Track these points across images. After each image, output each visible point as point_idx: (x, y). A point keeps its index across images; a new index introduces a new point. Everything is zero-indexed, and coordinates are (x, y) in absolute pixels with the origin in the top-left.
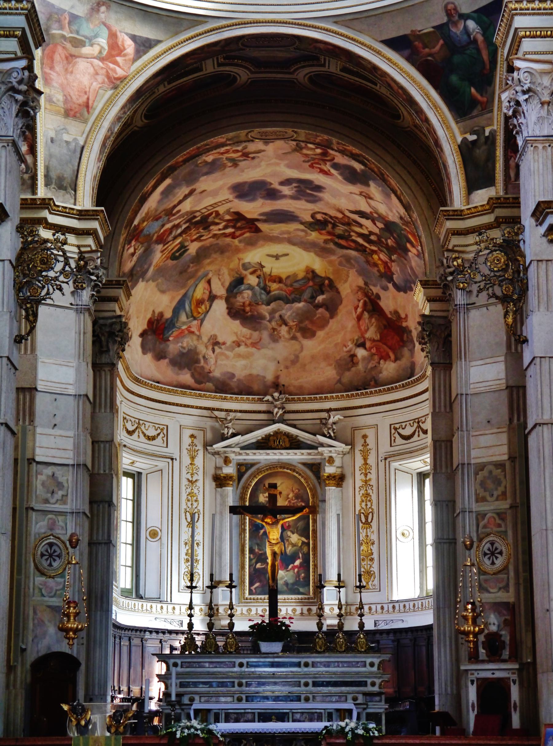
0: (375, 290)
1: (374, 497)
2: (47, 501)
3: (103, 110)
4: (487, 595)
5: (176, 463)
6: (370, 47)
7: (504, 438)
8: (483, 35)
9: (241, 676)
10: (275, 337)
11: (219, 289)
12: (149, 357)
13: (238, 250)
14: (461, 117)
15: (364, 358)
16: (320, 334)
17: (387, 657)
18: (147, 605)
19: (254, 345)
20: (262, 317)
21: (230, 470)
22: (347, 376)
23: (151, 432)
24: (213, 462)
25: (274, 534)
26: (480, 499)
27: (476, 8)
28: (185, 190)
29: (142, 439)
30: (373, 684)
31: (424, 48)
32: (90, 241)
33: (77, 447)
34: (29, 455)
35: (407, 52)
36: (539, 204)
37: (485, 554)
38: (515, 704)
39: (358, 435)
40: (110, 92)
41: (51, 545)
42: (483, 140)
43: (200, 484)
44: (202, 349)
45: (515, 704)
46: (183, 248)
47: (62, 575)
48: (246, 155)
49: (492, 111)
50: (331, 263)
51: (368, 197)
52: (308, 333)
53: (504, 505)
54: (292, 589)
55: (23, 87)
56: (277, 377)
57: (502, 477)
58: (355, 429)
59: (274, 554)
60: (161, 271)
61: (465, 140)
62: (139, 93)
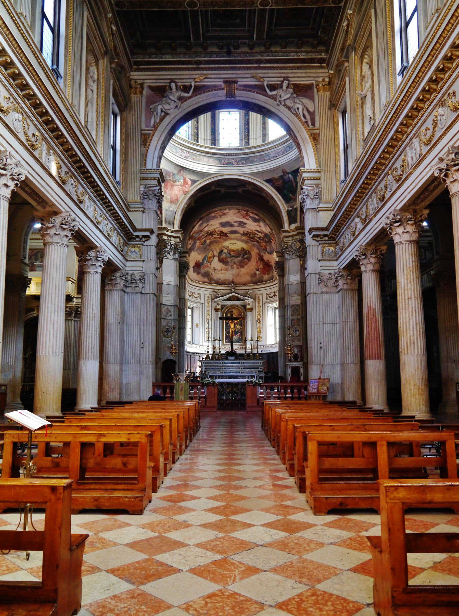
0: (262, 254)
1: (261, 315)
2: (166, 316)
3: (182, 201)
5: (203, 305)
6: (260, 182)
7: (299, 297)
9: (223, 366)
10: (232, 268)
11: (216, 253)
12: (195, 274)
13: (221, 242)
15: (258, 274)
16: (246, 267)
17: (265, 361)
18: (195, 346)
19: (226, 270)
20: (229, 262)
21: (219, 307)
22: (254, 279)
23: (196, 296)
24: (214, 304)
25: (232, 326)
26: (292, 315)
27: (291, 171)
28: (206, 224)
29: (194, 298)
30: (261, 368)
32: (178, 240)
33: (174, 300)
34: (161, 303)
35: (271, 184)
36: (310, 229)
39: (257, 296)
40: (184, 196)
41: (167, 328)
43: (210, 311)
44: (211, 271)
46: (205, 241)
47: (171, 337)
48: (224, 214)
50: (249, 246)
51: (260, 226)
52: (242, 266)
53: (299, 317)
54: (238, 341)
55: (159, 195)
56: (233, 280)
58: (256, 295)
59: (232, 331)
60: (199, 248)
61: (288, 209)
62: (192, 196)
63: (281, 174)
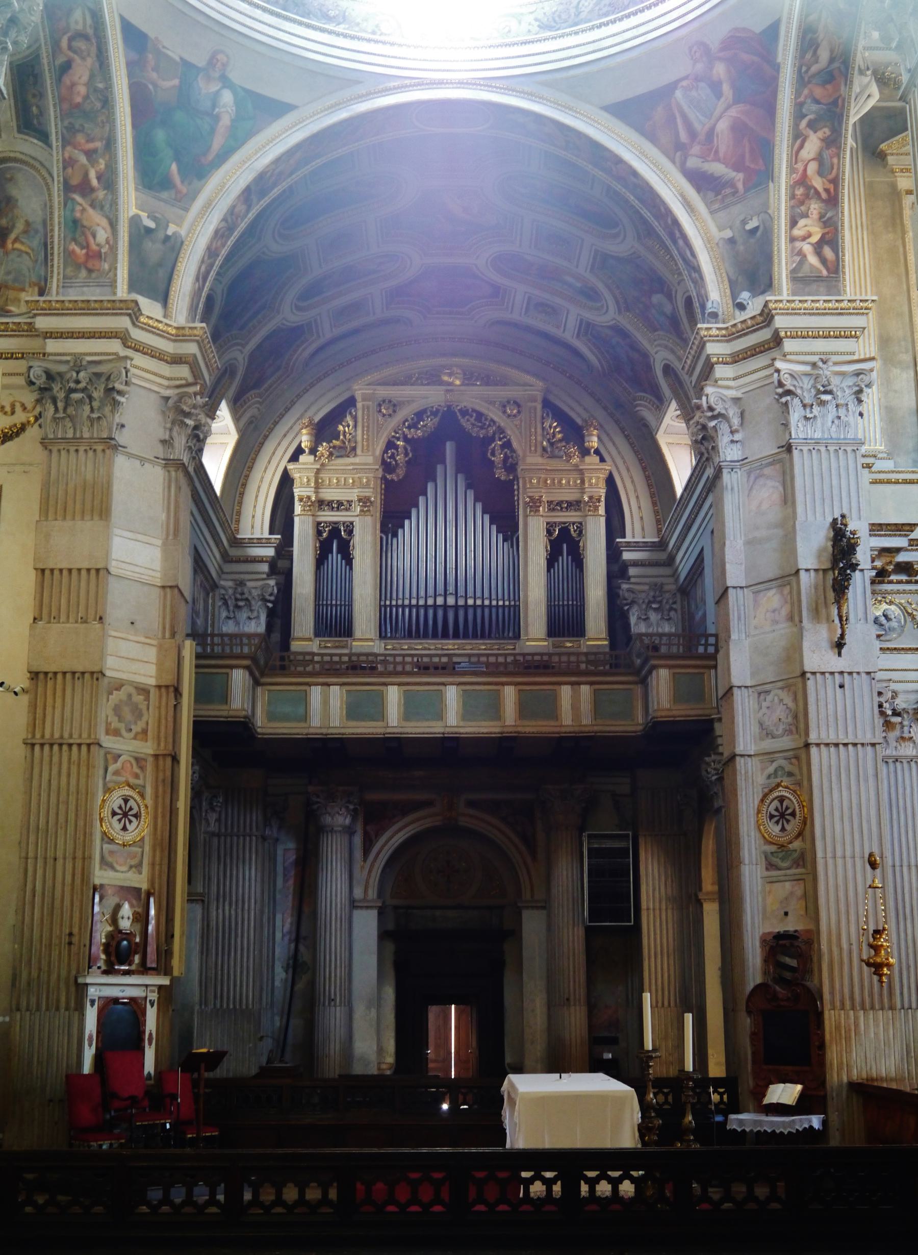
4: (111, 874)
7: (152, 654)
8: (233, 121)
14: (144, 187)
31: (153, 70)
37: (114, 814)
38: (151, 1034)
42: (161, 235)
45: (151, 1034)
49: (187, 210)
53: (147, 748)
57: (143, 707)
63: (200, 60)
